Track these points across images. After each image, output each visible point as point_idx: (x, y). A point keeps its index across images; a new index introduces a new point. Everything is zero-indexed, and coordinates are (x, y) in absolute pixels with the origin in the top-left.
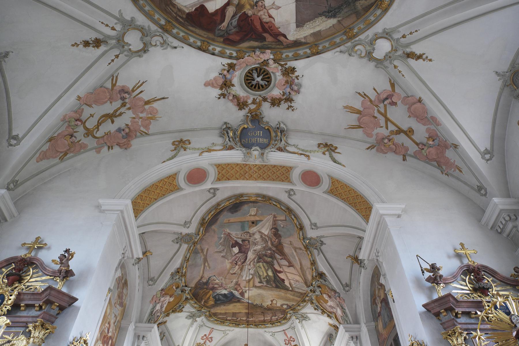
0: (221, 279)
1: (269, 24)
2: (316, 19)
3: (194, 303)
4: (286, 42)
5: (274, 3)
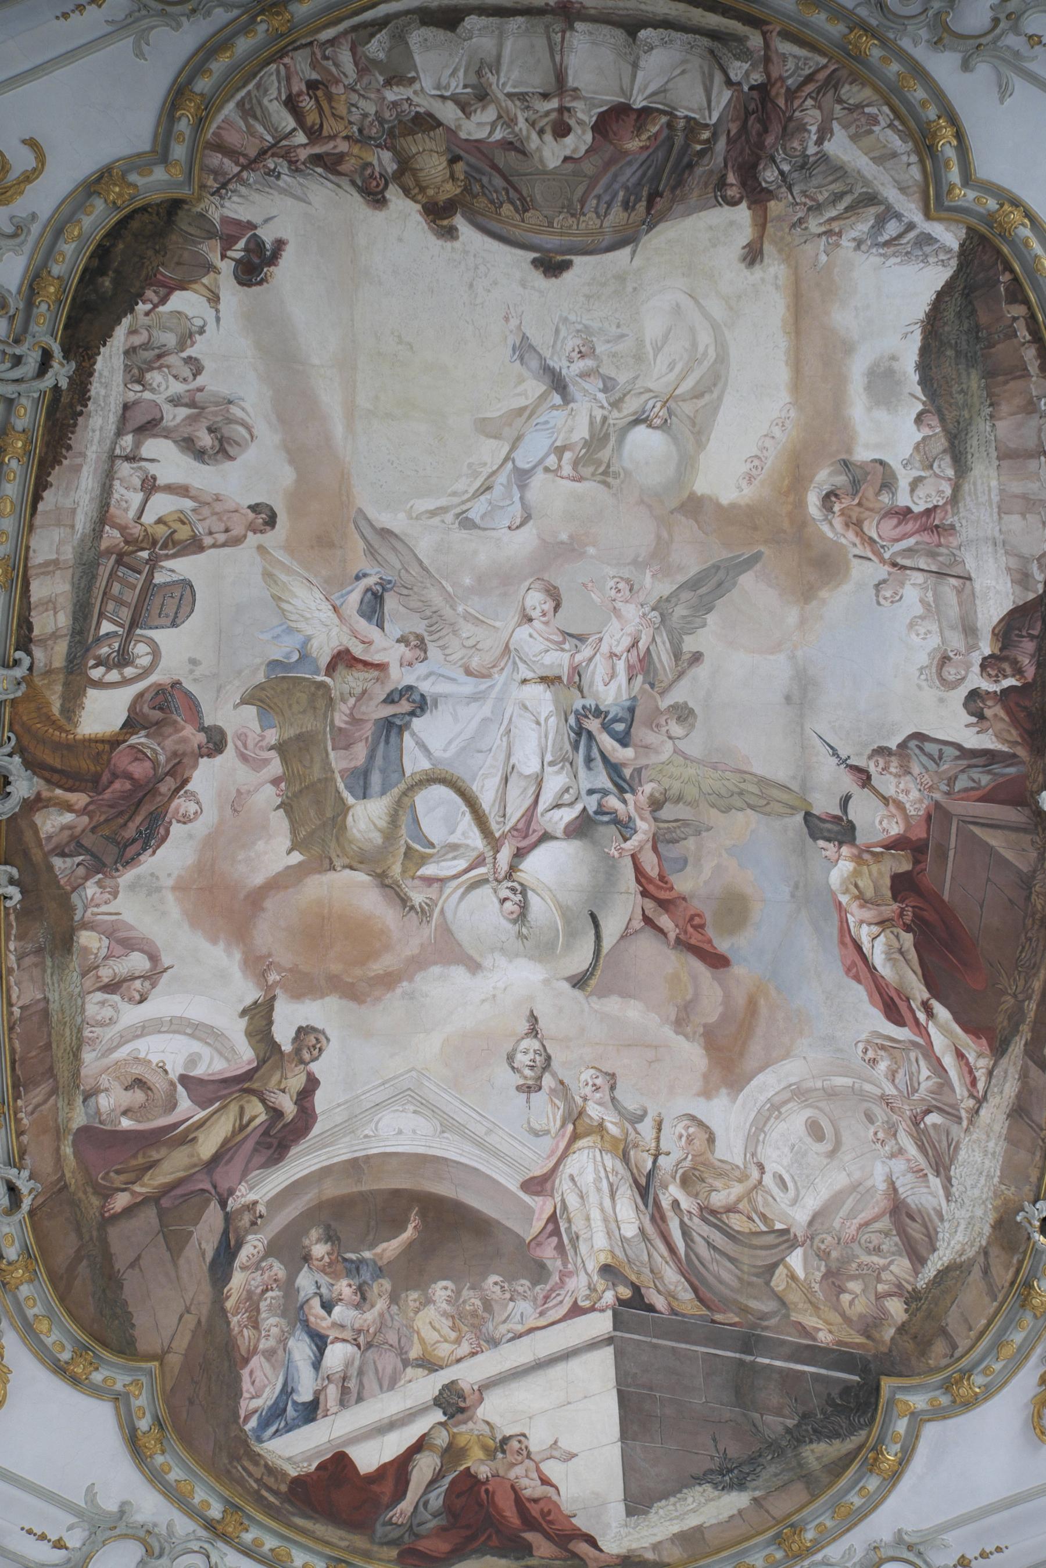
1: (542, 1504)
2: (685, 1491)
4: (596, 1560)
5: (556, 1443)
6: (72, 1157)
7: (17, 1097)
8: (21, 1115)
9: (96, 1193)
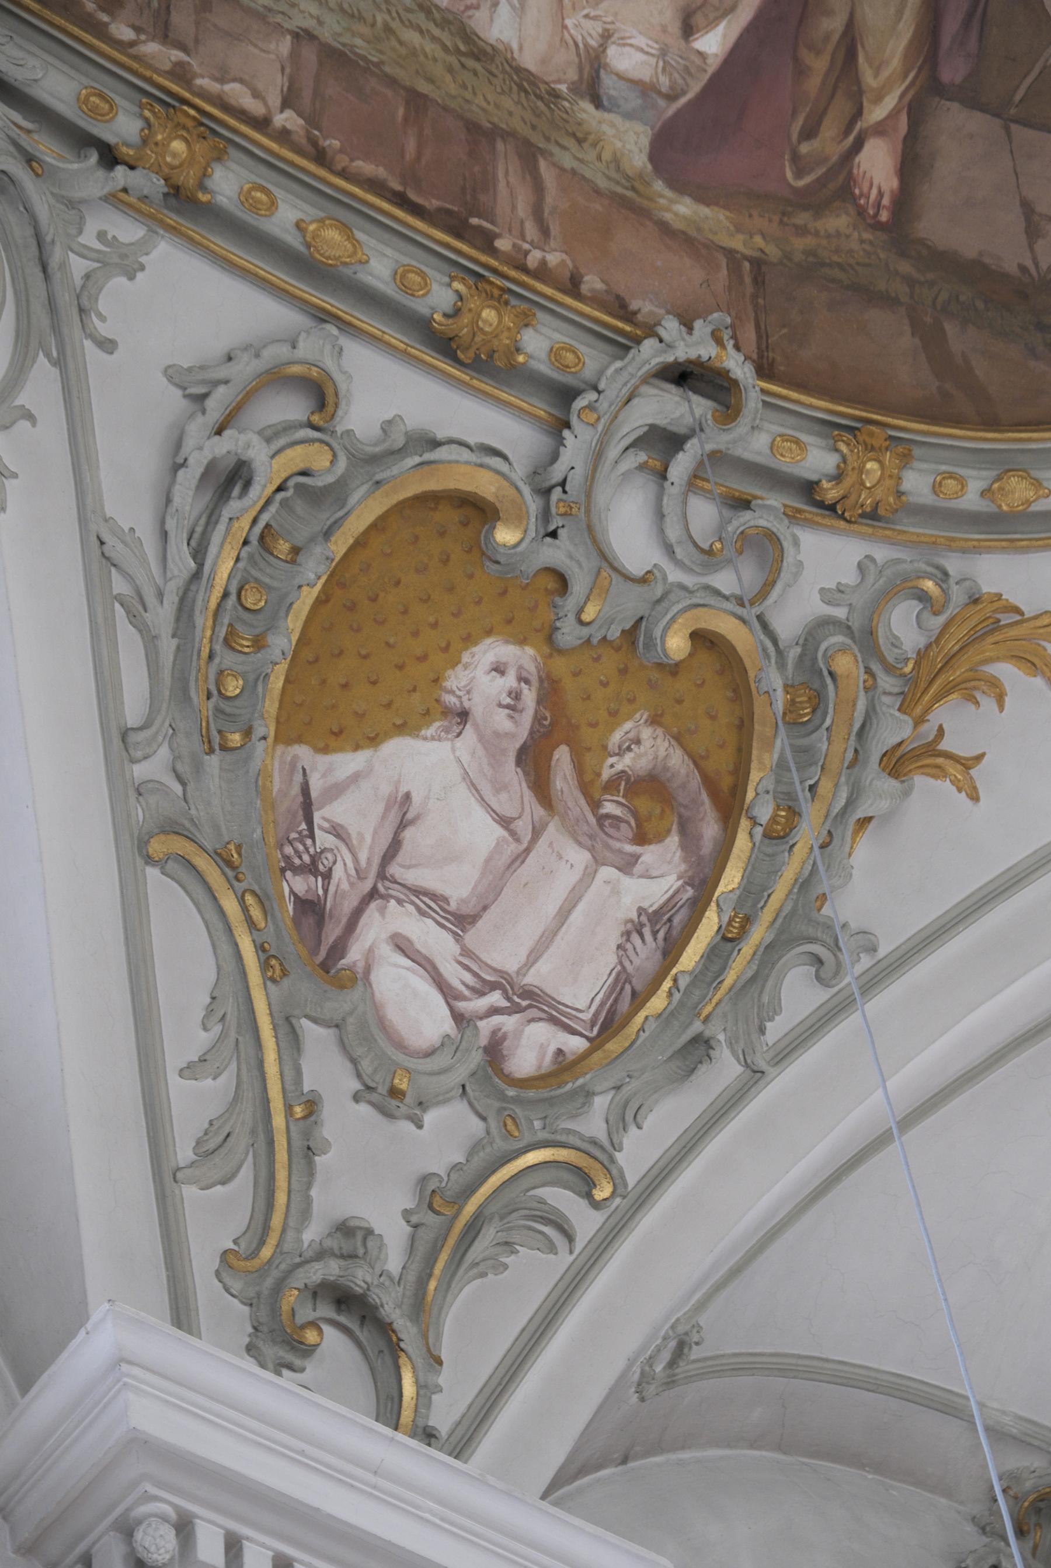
6: (705, 211)
7: (486, 242)
8: (534, 258)
9: (819, 209)
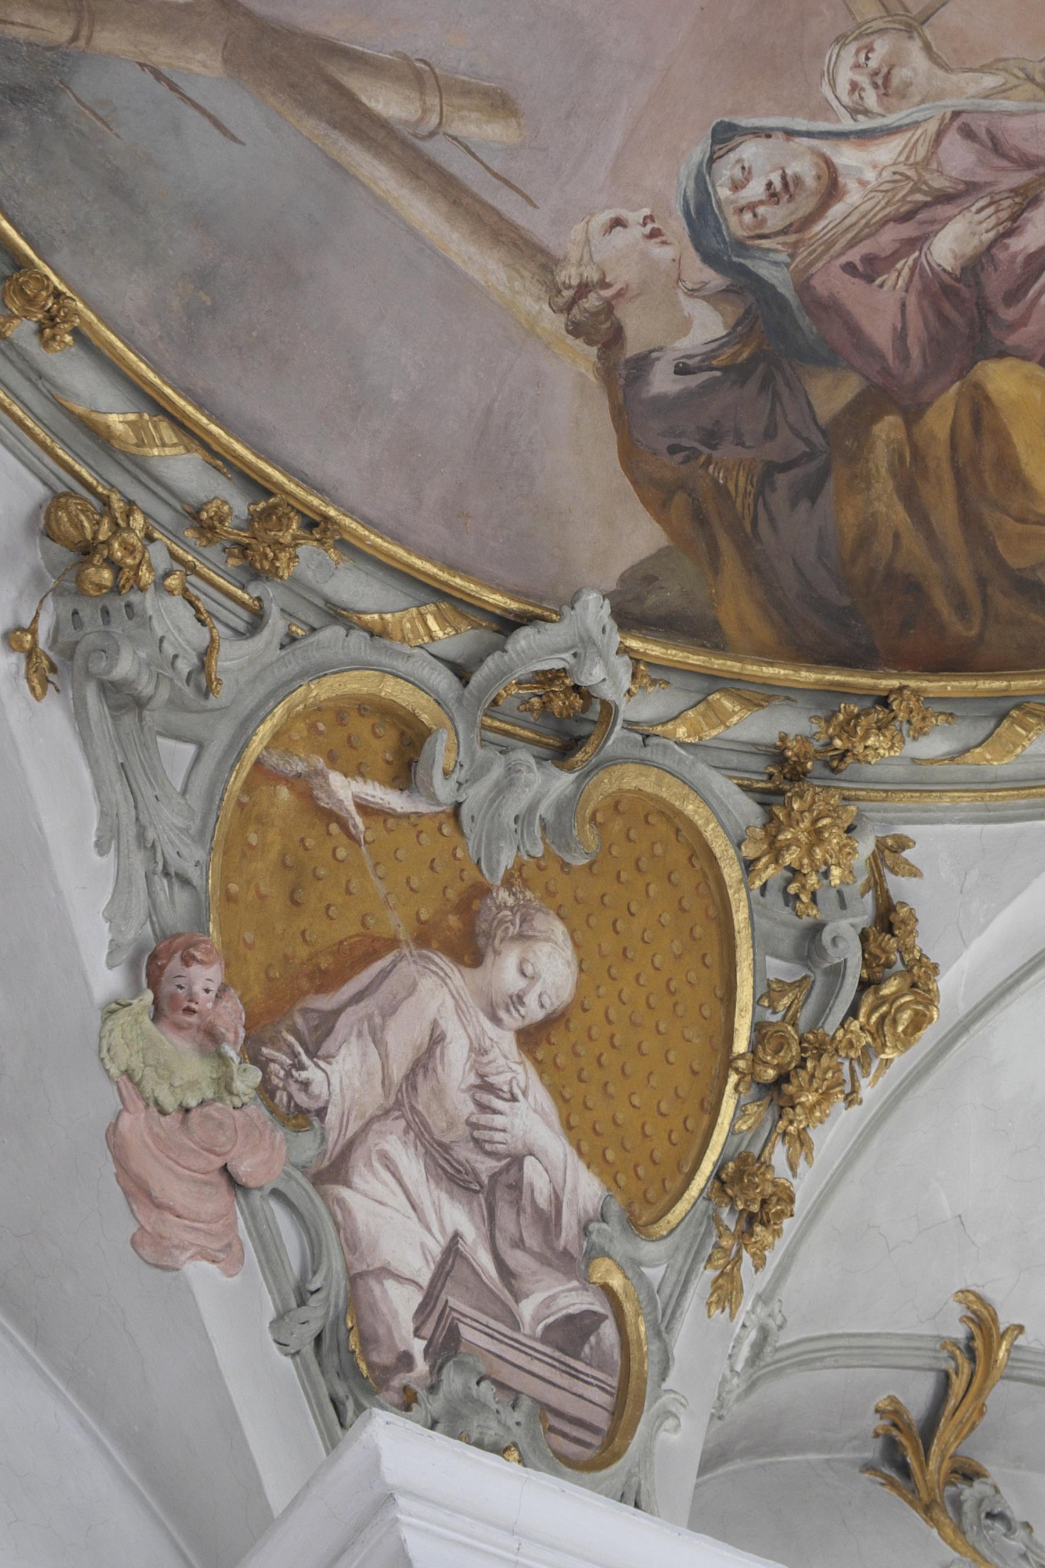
0: (883, 82)
3: (967, 732)
